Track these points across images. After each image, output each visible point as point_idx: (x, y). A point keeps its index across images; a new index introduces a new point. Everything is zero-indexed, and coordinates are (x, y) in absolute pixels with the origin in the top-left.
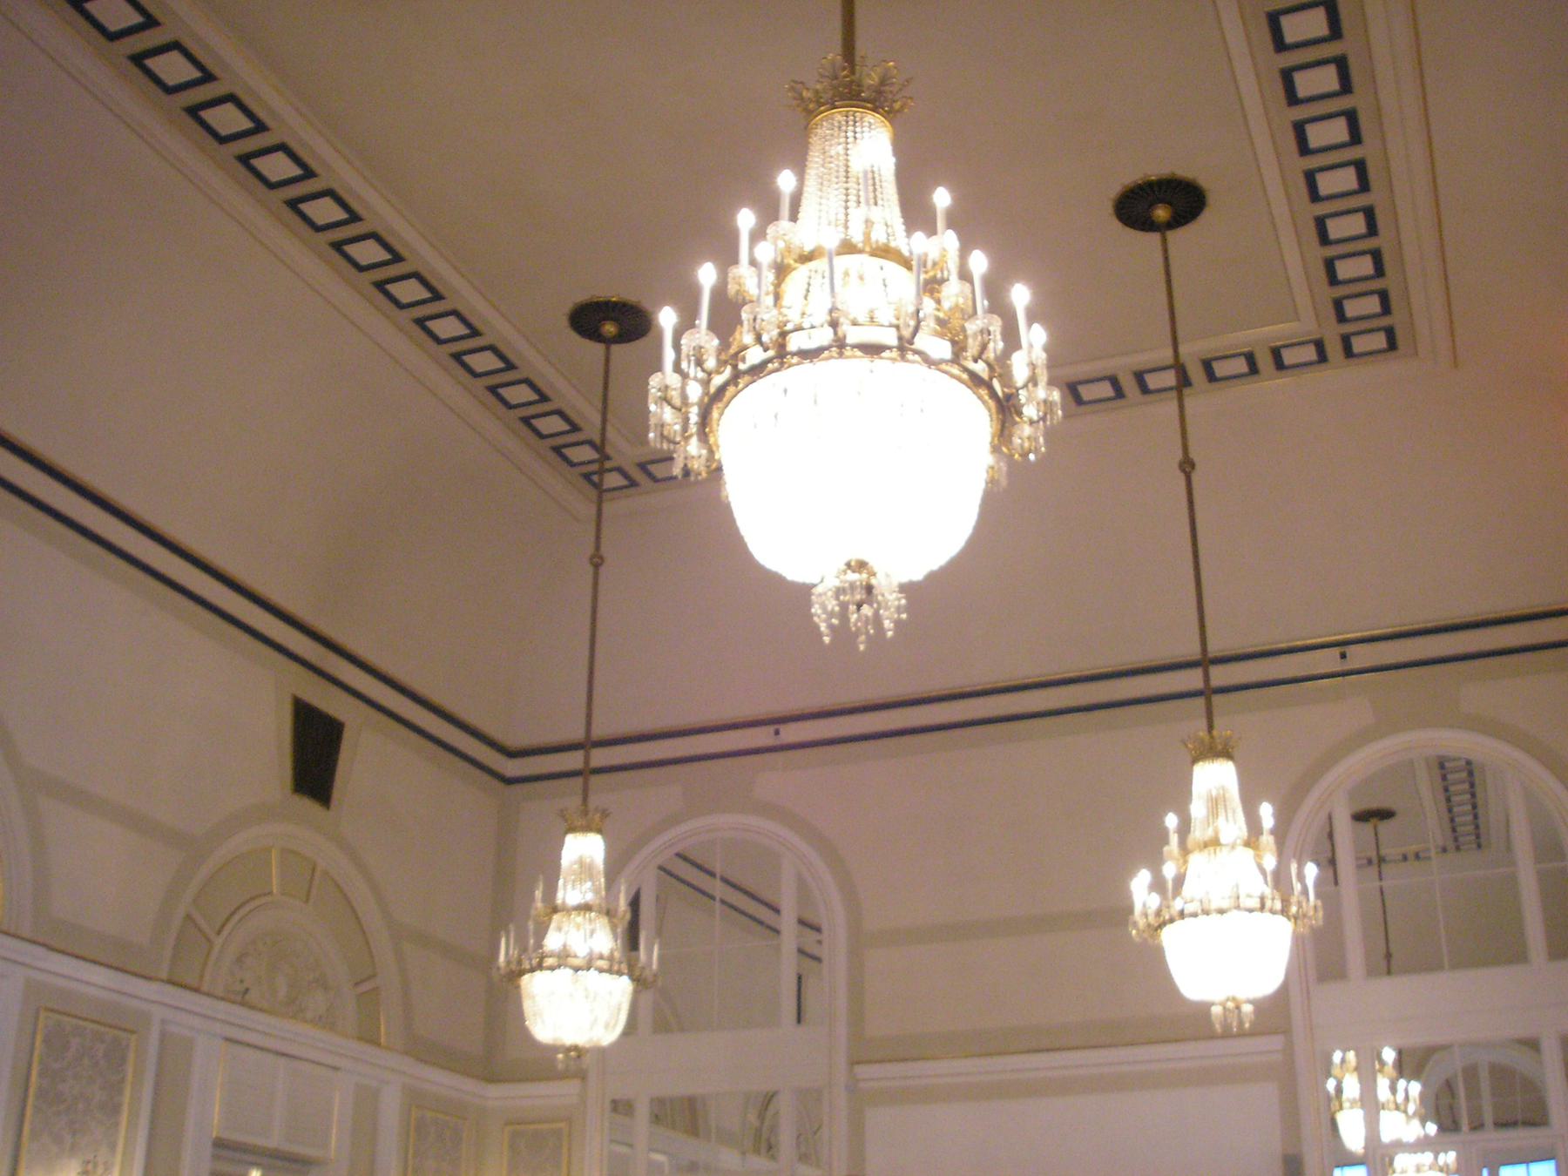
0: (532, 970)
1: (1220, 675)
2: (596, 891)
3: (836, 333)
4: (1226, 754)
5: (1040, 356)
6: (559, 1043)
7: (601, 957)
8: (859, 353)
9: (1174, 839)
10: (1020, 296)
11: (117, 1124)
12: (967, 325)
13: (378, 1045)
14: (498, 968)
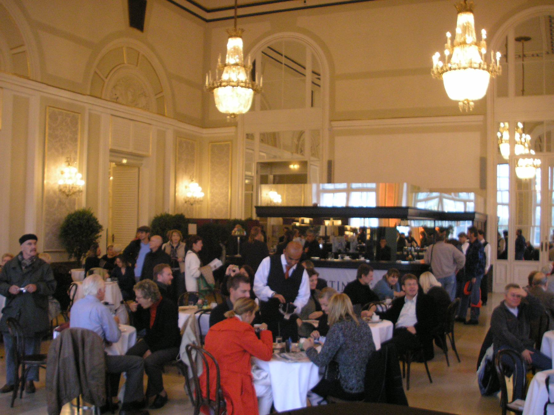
0: (218, 87)
2: (240, 59)
4: (470, 11)
7: (242, 82)
9: (449, 42)
11: (76, 145)
13: (164, 115)
14: (206, 86)
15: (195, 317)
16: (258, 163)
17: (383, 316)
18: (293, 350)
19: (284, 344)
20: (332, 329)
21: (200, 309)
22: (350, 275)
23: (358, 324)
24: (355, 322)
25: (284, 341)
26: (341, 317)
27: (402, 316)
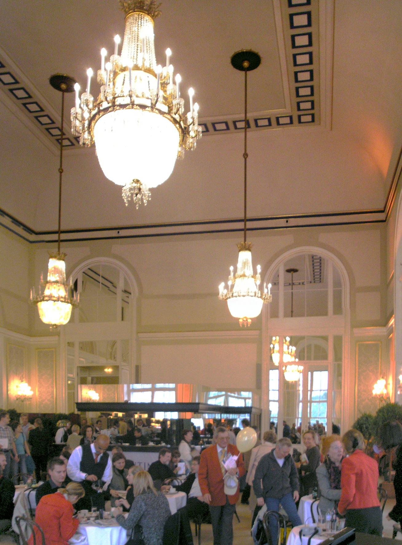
0: (41, 301)
1: (249, 225)
3: (131, 100)
4: (248, 249)
5: (196, 115)
6: (50, 323)
8: (138, 108)
10: (191, 92)
12: (173, 101)
14: (30, 300)
15: (24, 495)
16: (78, 367)
17: (179, 489)
18: (106, 517)
19: (98, 512)
20: (136, 500)
21: (29, 487)
22: (153, 457)
23: (157, 496)
24: (154, 494)
25: (98, 510)
26: (144, 490)
27: (193, 488)
